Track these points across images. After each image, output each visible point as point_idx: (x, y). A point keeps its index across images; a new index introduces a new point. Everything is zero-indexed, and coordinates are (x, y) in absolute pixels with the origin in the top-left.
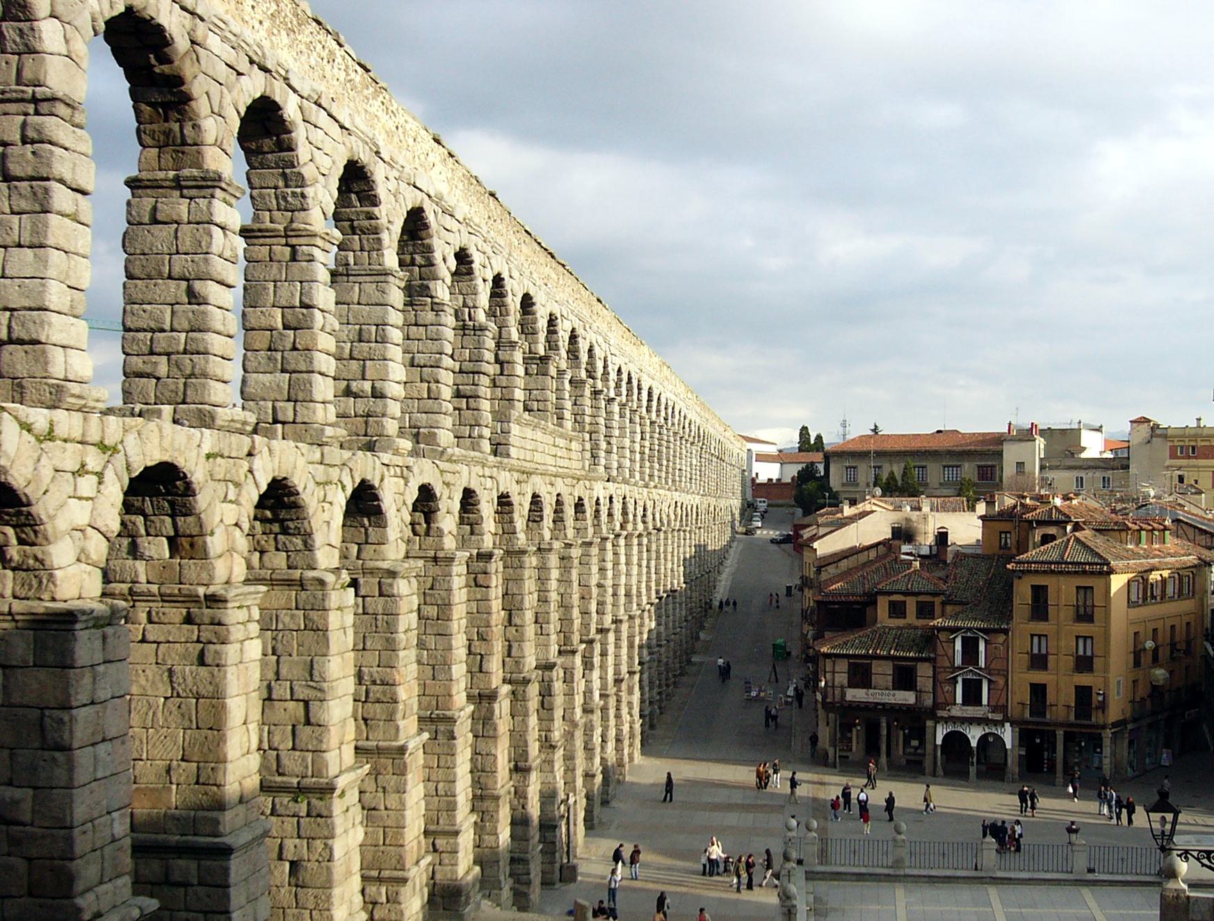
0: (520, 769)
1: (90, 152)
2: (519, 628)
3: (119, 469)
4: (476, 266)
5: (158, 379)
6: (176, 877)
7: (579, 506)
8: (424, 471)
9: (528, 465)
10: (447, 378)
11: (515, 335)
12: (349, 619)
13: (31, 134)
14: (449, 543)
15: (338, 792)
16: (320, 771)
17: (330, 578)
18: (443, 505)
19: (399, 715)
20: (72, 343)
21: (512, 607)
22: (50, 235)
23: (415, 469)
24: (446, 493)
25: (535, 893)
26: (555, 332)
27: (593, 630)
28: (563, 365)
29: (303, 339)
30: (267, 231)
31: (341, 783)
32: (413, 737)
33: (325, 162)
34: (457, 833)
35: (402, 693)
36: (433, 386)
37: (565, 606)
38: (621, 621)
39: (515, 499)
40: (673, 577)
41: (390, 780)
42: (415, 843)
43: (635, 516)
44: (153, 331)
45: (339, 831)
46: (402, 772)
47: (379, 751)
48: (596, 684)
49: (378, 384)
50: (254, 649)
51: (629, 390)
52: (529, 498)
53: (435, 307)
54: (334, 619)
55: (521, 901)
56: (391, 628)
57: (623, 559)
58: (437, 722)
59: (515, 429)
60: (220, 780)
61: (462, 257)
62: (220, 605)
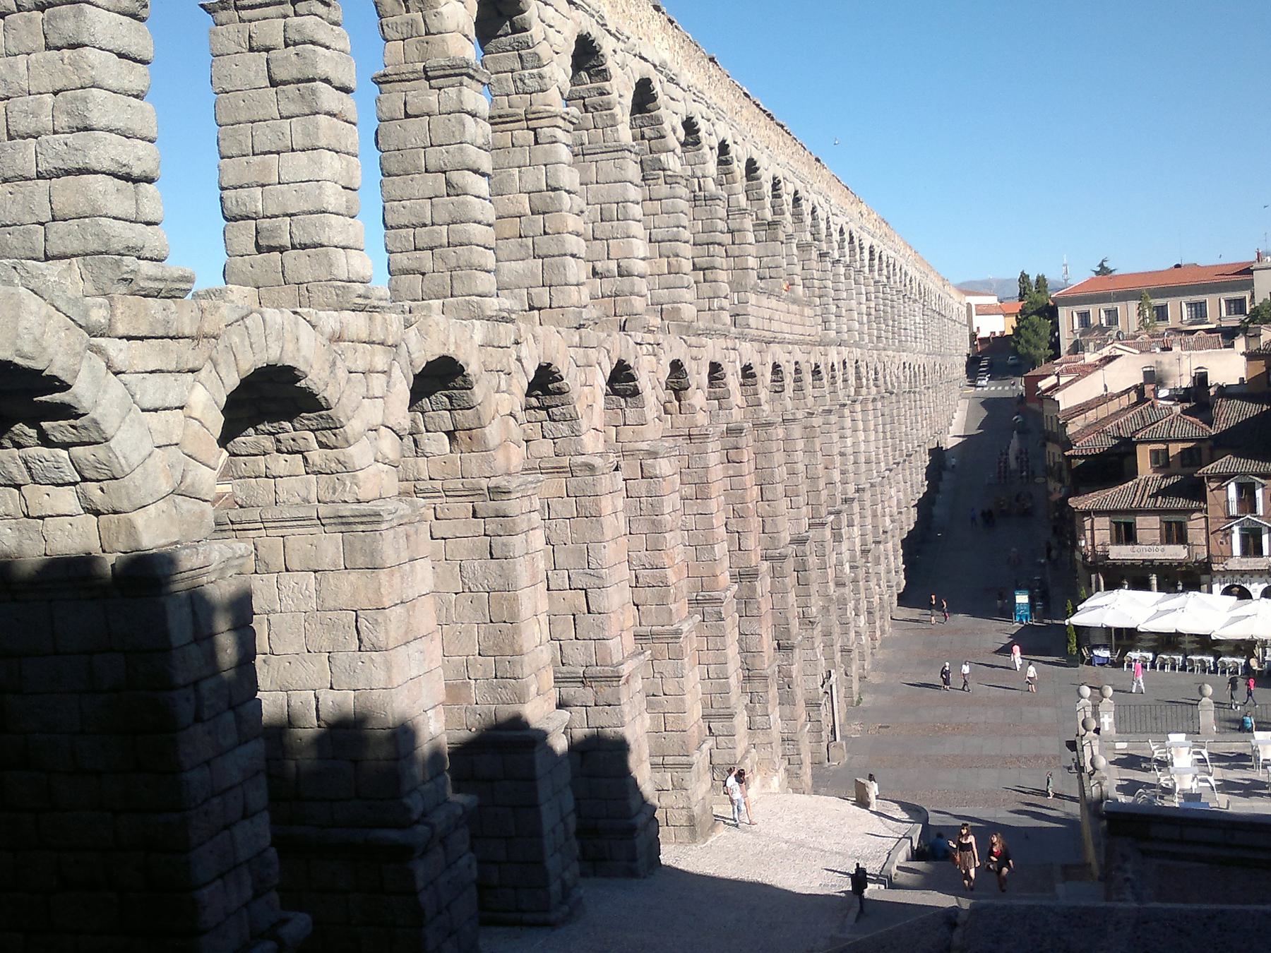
0: (783, 647)
1: (349, 49)
3: (404, 366)
4: (702, 134)
5: (423, 274)
7: (816, 372)
11: (743, 201)
12: (620, 503)
13: (294, 36)
15: (623, 680)
16: (604, 659)
17: (597, 461)
19: (671, 599)
20: (351, 244)
22: (321, 135)
23: (665, 345)
26: (779, 196)
27: (839, 501)
28: (790, 229)
29: (552, 222)
30: (508, 116)
31: (626, 669)
32: (685, 620)
34: (731, 716)
36: (673, 260)
38: (863, 490)
39: (757, 369)
41: (666, 666)
42: (695, 728)
48: (846, 556)
49: (623, 263)
50: (538, 539)
51: (852, 250)
53: (668, 180)
54: (606, 504)
56: (656, 511)
58: (703, 602)
60: (518, 673)
61: (690, 126)
62: (505, 497)
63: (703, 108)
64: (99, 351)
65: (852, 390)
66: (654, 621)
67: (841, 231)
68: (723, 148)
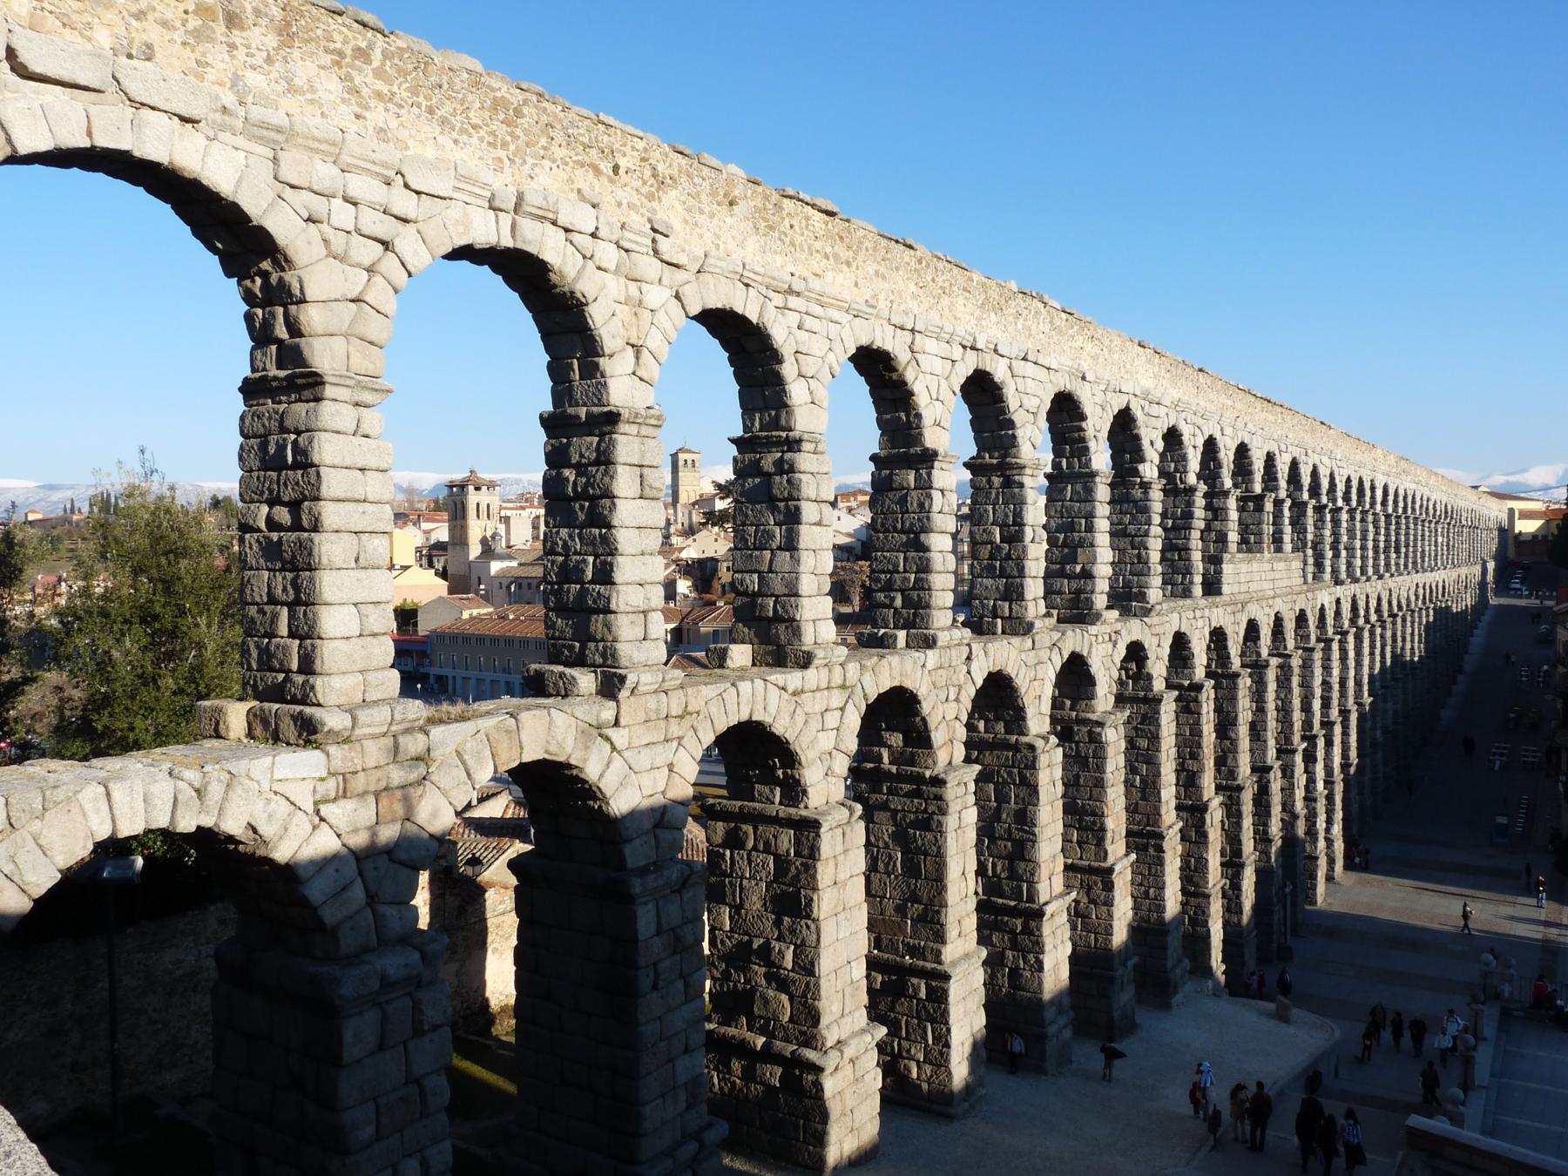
2: (1234, 742)
4: (1185, 438)
8: (1134, 630)
9: (1242, 597)
12: (1058, 773)
14: (1159, 685)
17: (1039, 743)
18: (1151, 654)
21: (1225, 725)
23: (1123, 632)
24: (1155, 641)
28: (1283, 494)
33: (1031, 403)
35: (1110, 823)
37: (1284, 711)
39: (1229, 631)
44: (891, 573)
45: (1048, 948)
46: (1109, 887)
47: (1090, 870)
50: (971, 816)
52: (1244, 625)
57: (1352, 654)
59: (1227, 568)
67: (1349, 480)
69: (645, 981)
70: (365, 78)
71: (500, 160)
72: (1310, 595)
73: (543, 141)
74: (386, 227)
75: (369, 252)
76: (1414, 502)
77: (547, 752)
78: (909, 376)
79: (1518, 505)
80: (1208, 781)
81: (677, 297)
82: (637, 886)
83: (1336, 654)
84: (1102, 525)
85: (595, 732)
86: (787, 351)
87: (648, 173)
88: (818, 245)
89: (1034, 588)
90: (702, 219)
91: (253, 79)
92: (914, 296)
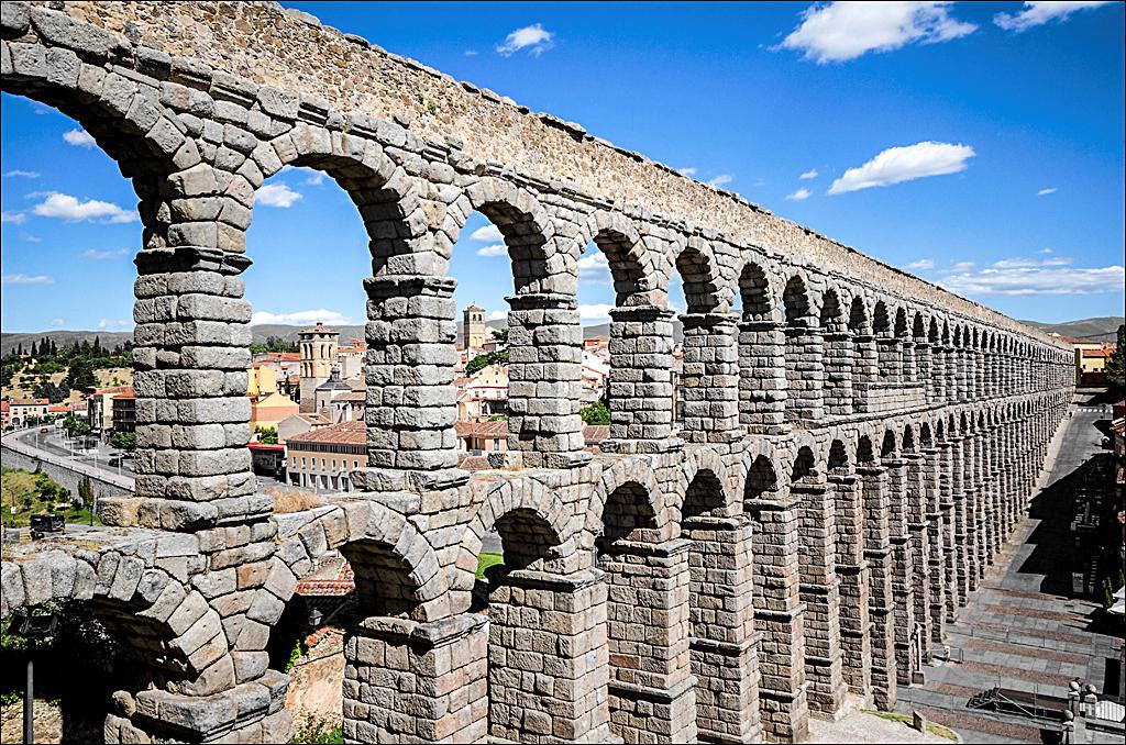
6: (641, 710)
8: (801, 437)
9: (881, 414)
10: (819, 375)
11: (870, 331)
12: (750, 545)
17: (735, 523)
18: (817, 458)
21: (871, 508)
23: (795, 440)
25: (893, 692)
28: (910, 339)
31: (743, 647)
34: (829, 664)
37: (913, 496)
40: (1007, 456)
43: (972, 423)
46: (788, 630)
49: (770, 392)
50: (686, 577)
54: (738, 548)
55: (881, 704)
57: (962, 456)
58: (813, 593)
63: (841, 282)
64: (414, 523)
65: (957, 432)
66: (775, 608)
67: (958, 328)
68: (857, 301)
69: (440, 706)
70: (231, 29)
71: (334, 92)
72: (930, 412)
73: (366, 79)
74: (246, 139)
75: (234, 158)
76: (1005, 345)
77: (367, 534)
78: (637, 250)
79: (1081, 347)
80: (859, 549)
81: (466, 193)
82: (434, 635)
83: (950, 456)
84: (780, 361)
85: (404, 518)
86: (547, 233)
87: (444, 102)
88: (570, 157)
89: (731, 408)
90: (484, 137)
91: (142, 26)
92: (641, 195)
